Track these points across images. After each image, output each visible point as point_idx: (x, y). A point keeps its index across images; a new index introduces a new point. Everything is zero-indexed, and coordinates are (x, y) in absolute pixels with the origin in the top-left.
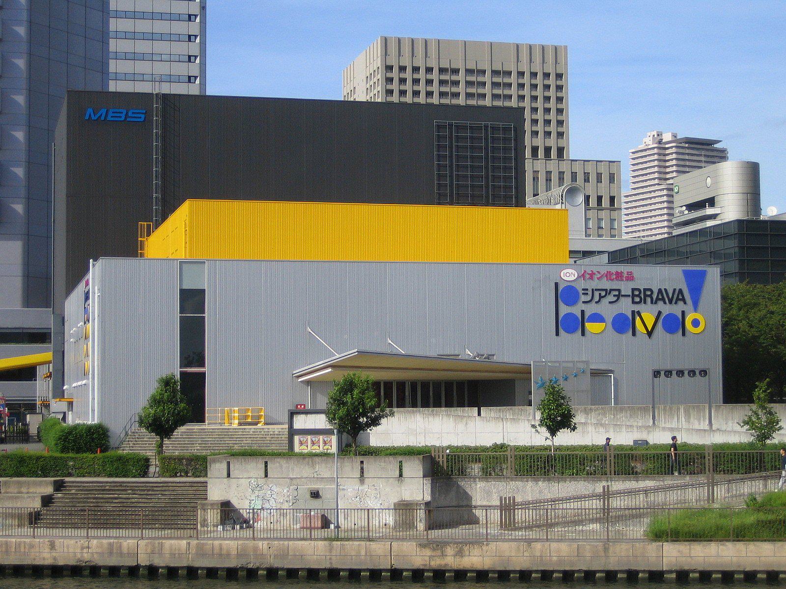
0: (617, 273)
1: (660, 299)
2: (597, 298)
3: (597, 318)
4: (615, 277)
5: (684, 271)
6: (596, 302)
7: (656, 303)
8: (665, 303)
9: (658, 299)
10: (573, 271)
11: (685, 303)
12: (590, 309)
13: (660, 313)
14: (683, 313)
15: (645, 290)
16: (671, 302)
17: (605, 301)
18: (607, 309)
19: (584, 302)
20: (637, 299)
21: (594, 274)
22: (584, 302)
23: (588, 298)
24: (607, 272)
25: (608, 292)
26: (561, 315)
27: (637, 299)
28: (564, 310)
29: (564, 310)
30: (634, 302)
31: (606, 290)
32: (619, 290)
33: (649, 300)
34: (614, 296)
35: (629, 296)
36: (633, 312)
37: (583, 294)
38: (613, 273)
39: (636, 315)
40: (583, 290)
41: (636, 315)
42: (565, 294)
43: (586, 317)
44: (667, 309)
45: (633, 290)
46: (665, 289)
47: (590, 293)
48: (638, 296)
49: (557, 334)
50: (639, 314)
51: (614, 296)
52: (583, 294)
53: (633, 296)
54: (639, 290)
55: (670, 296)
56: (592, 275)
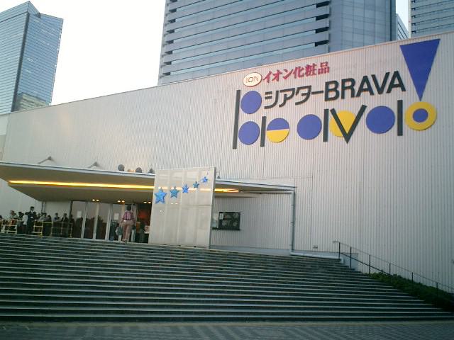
0: (308, 67)
1: (365, 90)
2: (281, 101)
3: (280, 124)
4: (304, 71)
6: (280, 106)
7: (359, 95)
8: (372, 93)
9: (361, 90)
11: (404, 89)
12: (272, 115)
13: (364, 108)
14: (400, 103)
15: (344, 81)
16: (380, 91)
19: (266, 108)
20: (332, 95)
22: (266, 108)
23: (271, 102)
24: (296, 68)
25: (295, 92)
26: (240, 126)
27: (332, 95)
28: (245, 118)
29: (245, 118)
30: (327, 99)
31: (293, 89)
32: (309, 87)
33: (348, 92)
34: (303, 95)
35: (322, 92)
36: (326, 111)
37: (266, 98)
40: (267, 93)
41: (330, 113)
43: (268, 123)
44: (372, 101)
46: (374, 76)
47: (274, 95)
48: (335, 89)
49: (235, 147)
50: (333, 111)
51: (303, 95)
52: (266, 98)
53: (328, 91)
54: (336, 83)
56: (277, 77)
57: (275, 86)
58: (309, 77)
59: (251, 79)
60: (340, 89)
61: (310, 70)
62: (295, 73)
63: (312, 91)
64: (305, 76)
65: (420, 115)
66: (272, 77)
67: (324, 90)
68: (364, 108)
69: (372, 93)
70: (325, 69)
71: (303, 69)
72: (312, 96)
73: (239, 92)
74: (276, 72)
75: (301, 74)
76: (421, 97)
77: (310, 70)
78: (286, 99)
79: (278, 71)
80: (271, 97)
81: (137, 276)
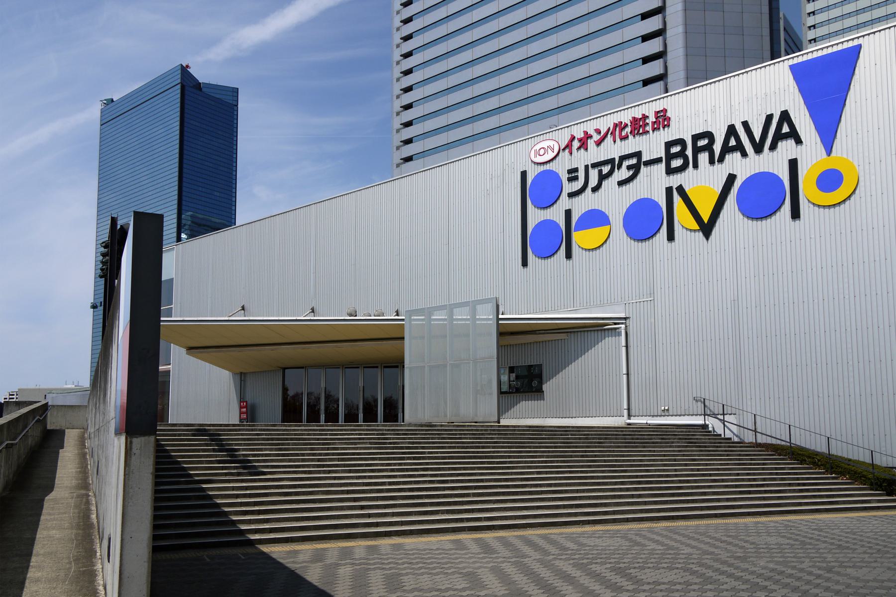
0: (635, 120)
2: (594, 180)
4: (628, 129)
5: (792, 67)
6: (595, 189)
7: (721, 159)
8: (744, 154)
9: (726, 149)
10: (551, 143)
11: (799, 141)
12: (581, 206)
13: (731, 178)
14: (793, 164)
15: (696, 138)
16: (758, 149)
17: (610, 184)
18: (614, 199)
19: (571, 195)
20: (677, 163)
21: (591, 137)
22: (571, 195)
23: (577, 185)
24: (616, 125)
27: (677, 163)
29: (535, 216)
30: (670, 171)
31: (611, 161)
32: (638, 155)
33: (704, 157)
35: (658, 161)
36: (669, 191)
38: (626, 125)
39: (677, 199)
40: (570, 172)
42: (537, 189)
45: (669, 145)
46: (745, 124)
47: (581, 174)
49: (525, 263)
50: (681, 190)
51: (629, 168)
53: (670, 157)
54: (681, 142)
55: (757, 136)
56: (583, 144)
57: (581, 159)
58: (637, 137)
59: (539, 149)
60: (689, 152)
61: (638, 126)
62: (613, 134)
63: (644, 159)
64: (631, 137)
65: (830, 180)
66: (576, 144)
67: (663, 155)
68: (731, 178)
69: (744, 154)
70: (662, 120)
71: (626, 125)
72: (643, 169)
73: (524, 174)
74: (582, 135)
75: (624, 134)
76: (829, 152)
77: (638, 126)
78: (602, 178)
79: (586, 133)
80: (576, 178)
81: (392, 470)
